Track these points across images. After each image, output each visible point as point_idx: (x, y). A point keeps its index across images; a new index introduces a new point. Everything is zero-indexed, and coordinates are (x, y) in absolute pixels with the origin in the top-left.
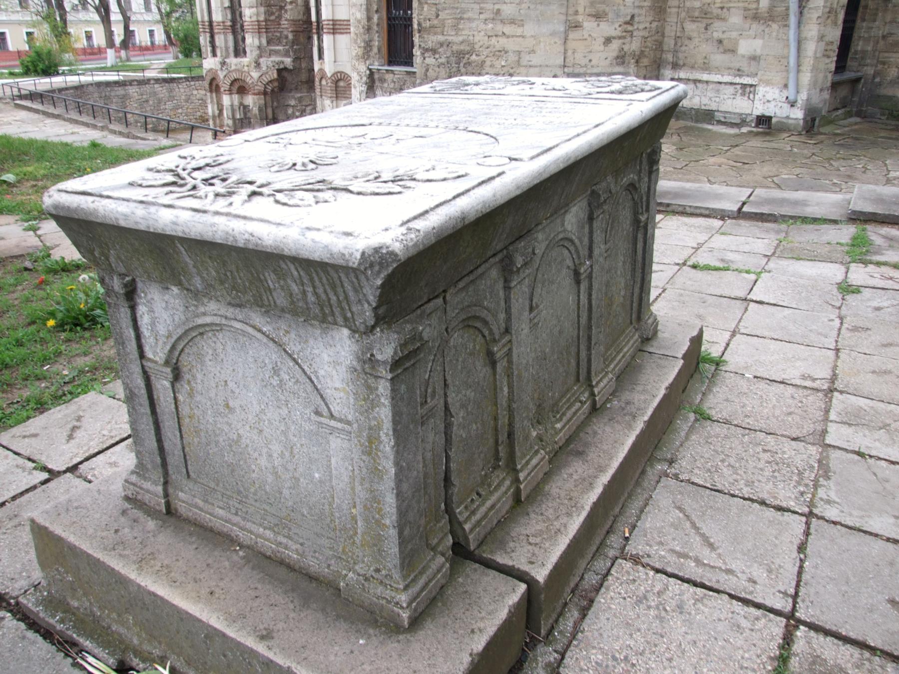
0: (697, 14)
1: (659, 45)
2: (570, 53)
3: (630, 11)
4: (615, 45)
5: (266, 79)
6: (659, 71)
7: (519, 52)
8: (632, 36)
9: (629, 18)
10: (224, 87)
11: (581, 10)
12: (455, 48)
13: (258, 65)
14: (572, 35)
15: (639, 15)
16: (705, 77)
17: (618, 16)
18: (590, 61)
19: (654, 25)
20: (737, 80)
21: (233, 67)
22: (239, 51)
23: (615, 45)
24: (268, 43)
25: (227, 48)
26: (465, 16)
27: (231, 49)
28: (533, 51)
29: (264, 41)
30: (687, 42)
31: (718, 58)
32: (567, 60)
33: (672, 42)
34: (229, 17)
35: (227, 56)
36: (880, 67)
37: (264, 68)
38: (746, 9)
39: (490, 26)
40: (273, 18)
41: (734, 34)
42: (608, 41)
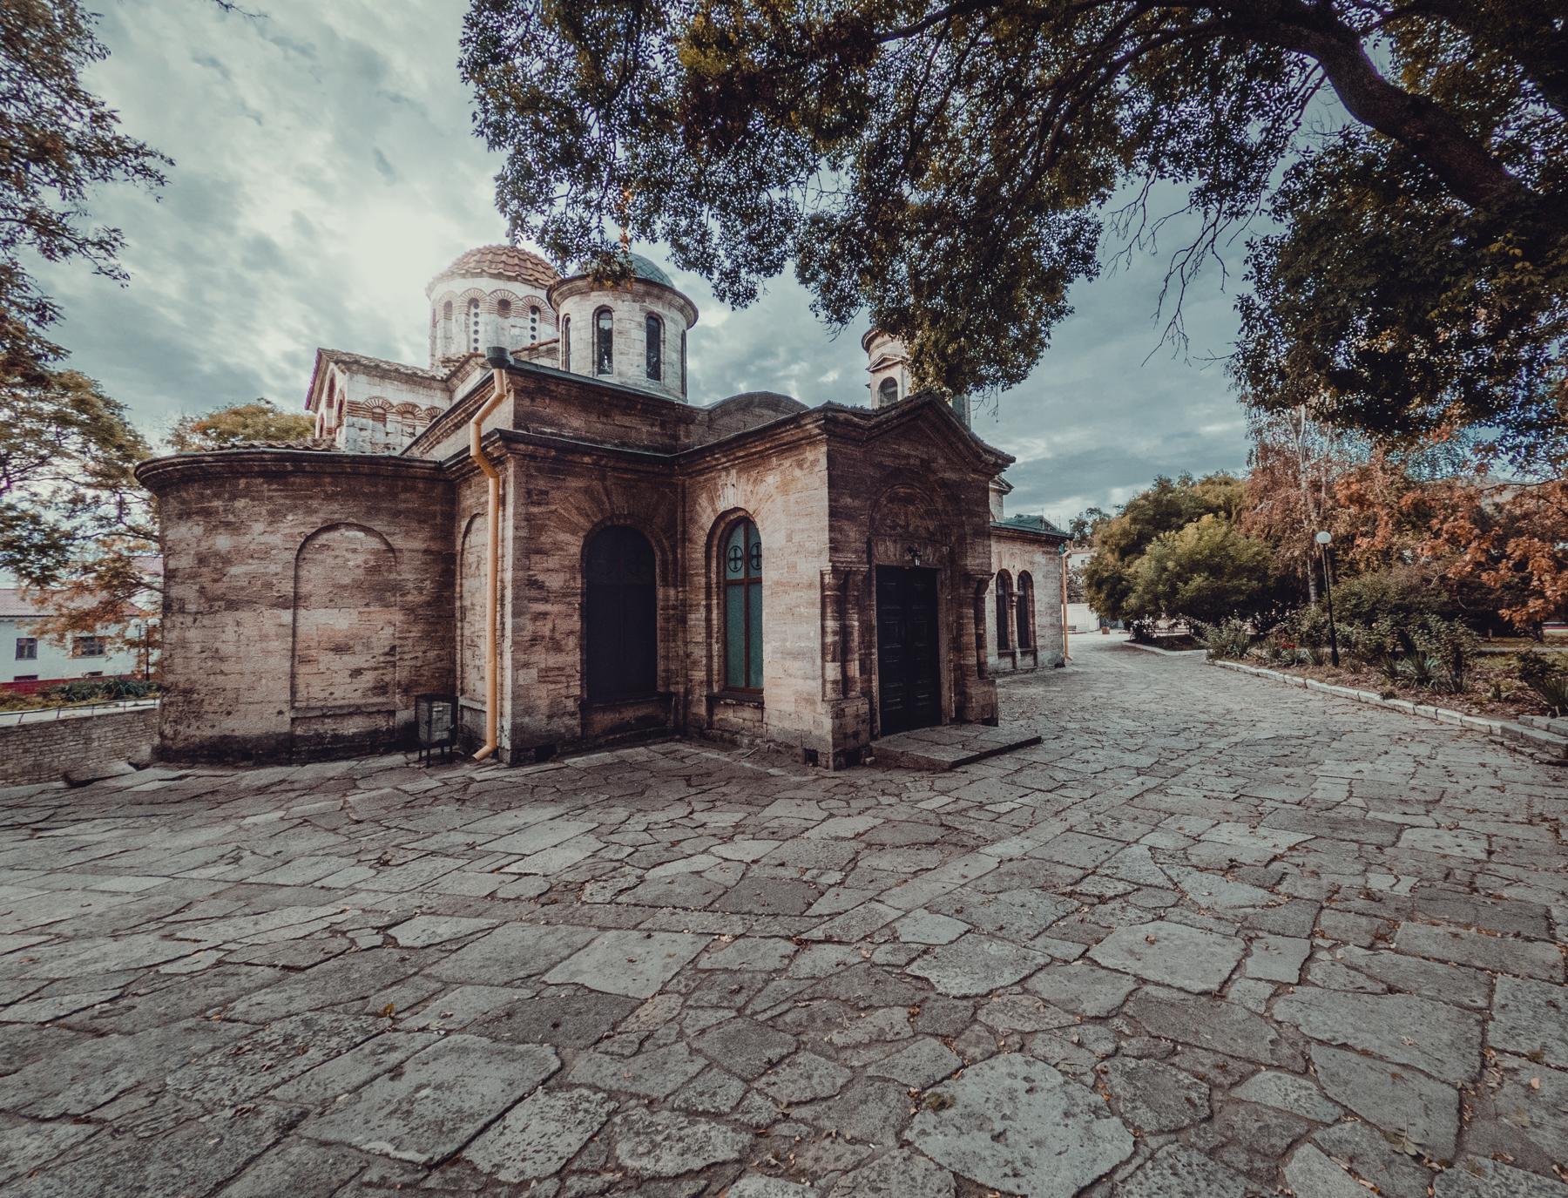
2: (301, 688)
4: (368, 679)
8: (394, 666)
19: (432, 654)
42: (357, 672)
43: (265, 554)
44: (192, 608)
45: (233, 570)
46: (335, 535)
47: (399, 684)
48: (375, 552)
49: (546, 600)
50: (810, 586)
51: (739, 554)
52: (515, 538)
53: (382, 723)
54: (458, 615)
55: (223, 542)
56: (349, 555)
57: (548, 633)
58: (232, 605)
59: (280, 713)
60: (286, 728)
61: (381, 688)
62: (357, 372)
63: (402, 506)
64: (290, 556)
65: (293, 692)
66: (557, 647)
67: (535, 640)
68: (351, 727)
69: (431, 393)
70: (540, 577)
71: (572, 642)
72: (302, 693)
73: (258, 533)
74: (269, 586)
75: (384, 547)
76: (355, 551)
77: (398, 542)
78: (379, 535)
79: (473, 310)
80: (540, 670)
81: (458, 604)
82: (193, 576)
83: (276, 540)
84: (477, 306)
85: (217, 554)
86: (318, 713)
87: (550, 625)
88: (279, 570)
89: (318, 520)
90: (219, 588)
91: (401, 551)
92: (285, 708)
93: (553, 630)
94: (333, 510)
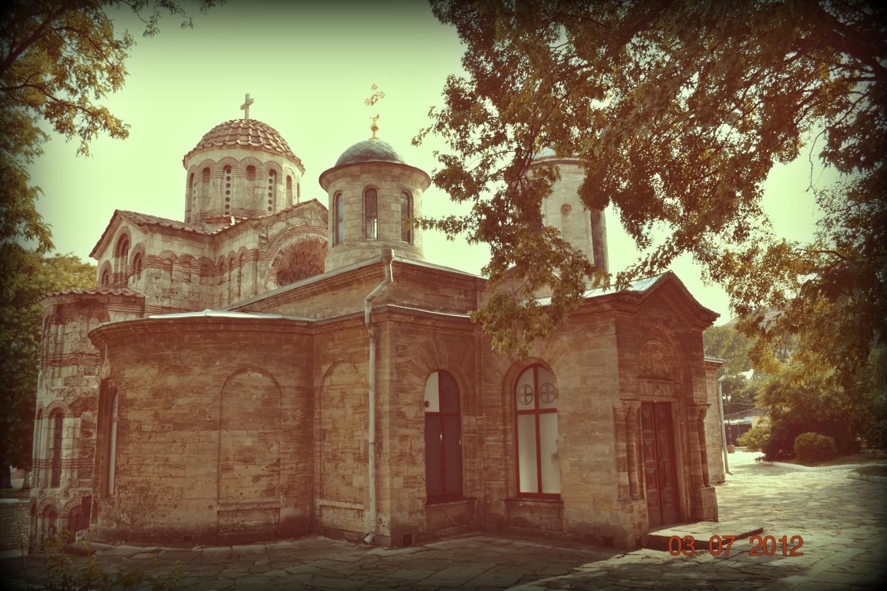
0: (330, 457)
1: (311, 479)
2: (223, 488)
3: (276, 456)
4: (264, 482)
5: (71, 505)
6: (313, 500)
7: (182, 488)
9: (275, 461)
10: (40, 512)
11: (231, 457)
12: (138, 485)
13: (67, 494)
14: (224, 476)
15: (284, 459)
16: (337, 504)
17: (264, 460)
18: (242, 494)
19: (301, 465)
20: (354, 506)
21: (48, 496)
22: (55, 483)
23: (264, 482)
24: (79, 476)
25: (46, 480)
26: (145, 463)
27: (50, 481)
28: (192, 488)
29: (75, 475)
30: (327, 478)
31: (344, 489)
32: (221, 494)
33: (319, 477)
34: (52, 456)
35: (46, 486)
36: (488, 492)
37: (72, 497)
38: (354, 454)
39: (162, 469)
40: (86, 456)
41: (350, 471)
42: (257, 478)
43: (200, 390)
44: (147, 428)
45: (180, 401)
46: (244, 376)
47: (282, 488)
48: (268, 389)
49: (406, 426)
50: (605, 417)
51: (529, 391)
52: (391, 381)
53: (272, 519)
54: (316, 436)
55: (172, 380)
56: (252, 391)
57: (408, 451)
58: (178, 427)
59: (210, 507)
60: (215, 519)
61: (270, 491)
62: (155, 232)
63: (284, 354)
64: (217, 392)
65: (219, 493)
66: (413, 462)
67: (402, 455)
68: (255, 520)
69: (202, 245)
70: (404, 409)
71: (420, 458)
72: (223, 493)
73: (197, 375)
74: (204, 413)
75: (273, 385)
76: (256, 388)
77: (282, 381)
78: (271, 376)
79: (226, 175)
80: (405, 478)
81: (317, 427)
82: (149, 405)
83: (209, 379)
84: (229, 172)
85: (168, 389)
86: (234, 508)
87: (409, 446)
88: (210, 401)
89: (234, 364)
90: (170, 414)
91: (284, 387)
92: (214, 503)
93: (411, 448)
94: (243, 357)
